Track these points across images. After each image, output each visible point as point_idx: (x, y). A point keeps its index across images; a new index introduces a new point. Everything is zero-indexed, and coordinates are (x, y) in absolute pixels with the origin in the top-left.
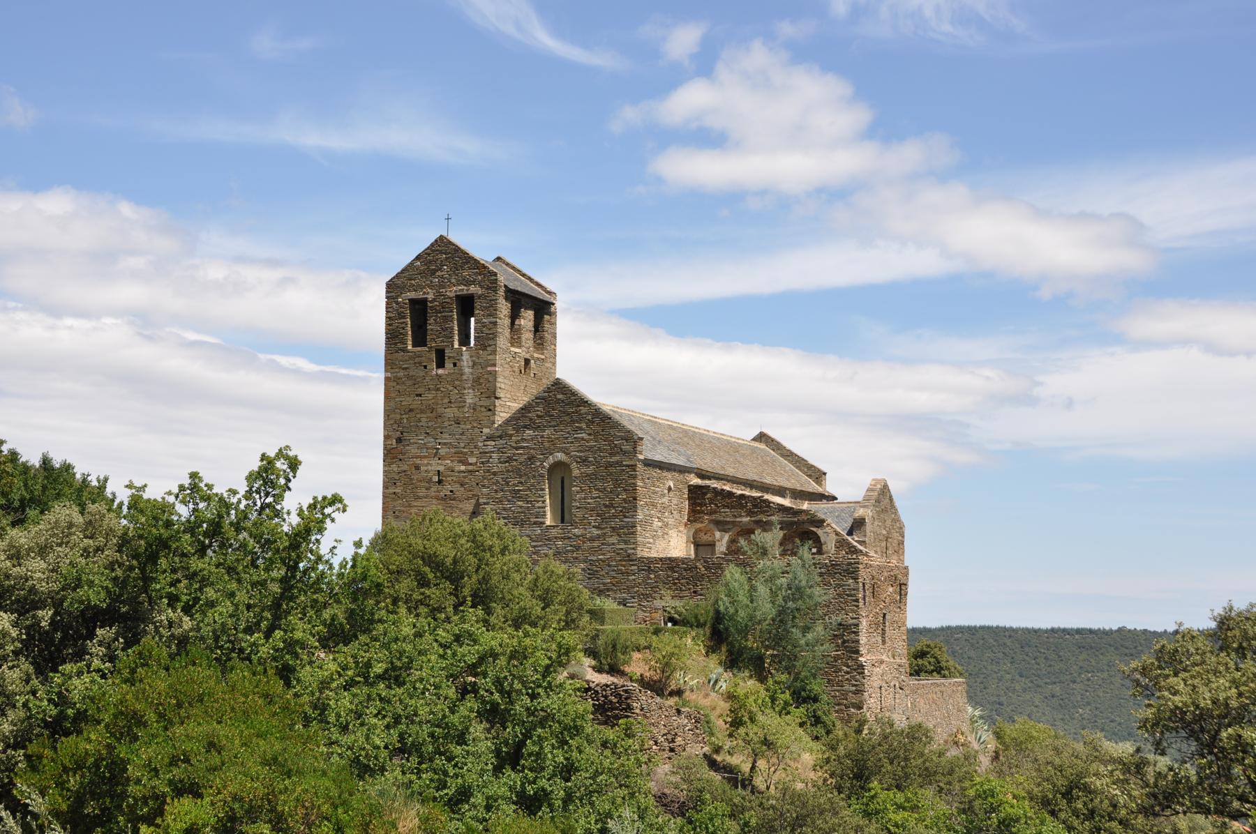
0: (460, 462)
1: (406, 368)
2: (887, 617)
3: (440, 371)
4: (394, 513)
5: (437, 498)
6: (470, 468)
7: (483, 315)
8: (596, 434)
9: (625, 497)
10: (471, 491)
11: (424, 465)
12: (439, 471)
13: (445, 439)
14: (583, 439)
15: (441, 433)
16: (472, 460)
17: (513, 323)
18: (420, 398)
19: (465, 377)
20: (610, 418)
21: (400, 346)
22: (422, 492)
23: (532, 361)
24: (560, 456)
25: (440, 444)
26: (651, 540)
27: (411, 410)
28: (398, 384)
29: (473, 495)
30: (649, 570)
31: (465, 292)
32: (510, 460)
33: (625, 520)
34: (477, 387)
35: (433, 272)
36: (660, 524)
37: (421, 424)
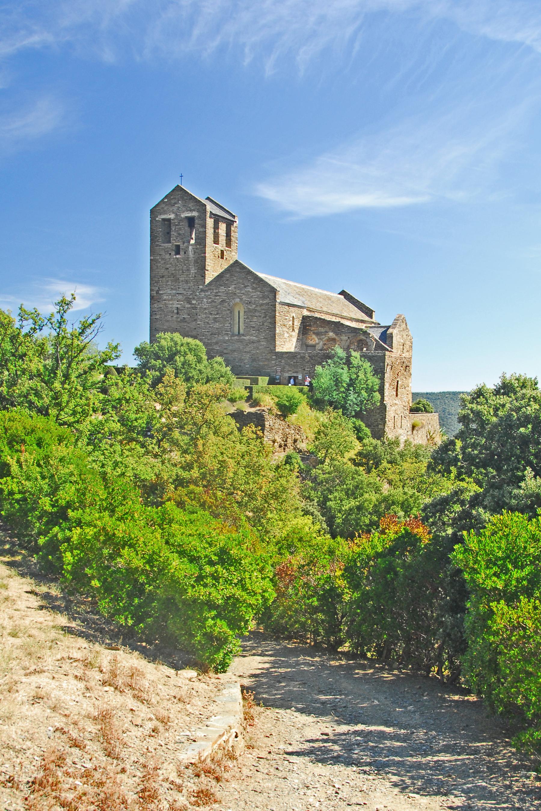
0: (187, 303)
1: (160, 255)
2: (399, 383)
3: (178, 256)
6: (193, 306)
14: (249, 291)
16: (194, 302)
17: (215, 231)
19: (190, 259)
23: (225, 252)
25: (178, 294)
26: (283, 343)
27: (163, 277)
30: (282, 358)
31: (190, 215)
32: (213, 301)
36: (288, 335)
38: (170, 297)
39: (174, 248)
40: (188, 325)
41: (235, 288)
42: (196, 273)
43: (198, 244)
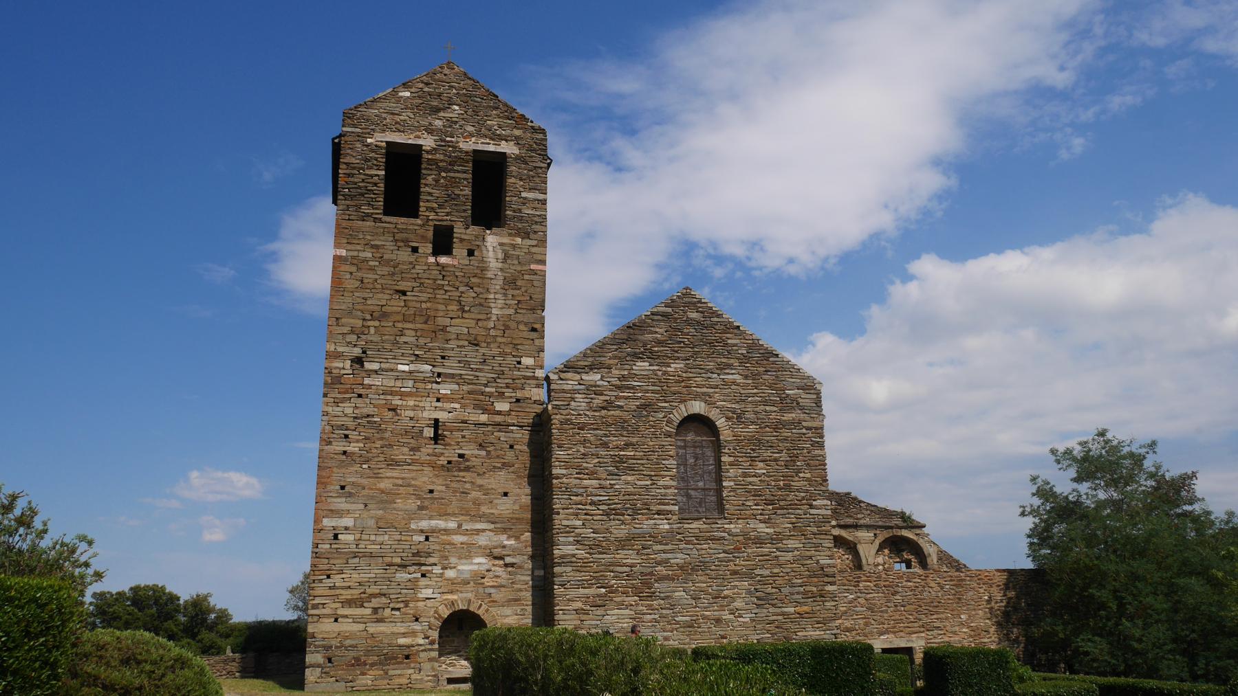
0: (476, 407)
1: (377, 247)
3: (443, 260)
4: (343, 488)
5: (433, 466)
7: (521, 186)
8: (755, 376)
9: (808, 475)
11: (406, 408)
12: (437, 421)
13: (451, 368)
14: (734, 383)
15: (443, 357)
18: (404, 298)
19: (490, 275)
20: (777, 355)
22: (402, 453)
24: (697, 407)
25: (439, 375)
27: (384, 316)
28: (359, 269)
29: (504, 464)
31: (491, 148)
32: (608, 405)
33: (813, 511)
34: (511, 292)
35: (436, 110)
38: (410, 383)
39: (430, 234)
40: (479, 481)
43: (518, 235)
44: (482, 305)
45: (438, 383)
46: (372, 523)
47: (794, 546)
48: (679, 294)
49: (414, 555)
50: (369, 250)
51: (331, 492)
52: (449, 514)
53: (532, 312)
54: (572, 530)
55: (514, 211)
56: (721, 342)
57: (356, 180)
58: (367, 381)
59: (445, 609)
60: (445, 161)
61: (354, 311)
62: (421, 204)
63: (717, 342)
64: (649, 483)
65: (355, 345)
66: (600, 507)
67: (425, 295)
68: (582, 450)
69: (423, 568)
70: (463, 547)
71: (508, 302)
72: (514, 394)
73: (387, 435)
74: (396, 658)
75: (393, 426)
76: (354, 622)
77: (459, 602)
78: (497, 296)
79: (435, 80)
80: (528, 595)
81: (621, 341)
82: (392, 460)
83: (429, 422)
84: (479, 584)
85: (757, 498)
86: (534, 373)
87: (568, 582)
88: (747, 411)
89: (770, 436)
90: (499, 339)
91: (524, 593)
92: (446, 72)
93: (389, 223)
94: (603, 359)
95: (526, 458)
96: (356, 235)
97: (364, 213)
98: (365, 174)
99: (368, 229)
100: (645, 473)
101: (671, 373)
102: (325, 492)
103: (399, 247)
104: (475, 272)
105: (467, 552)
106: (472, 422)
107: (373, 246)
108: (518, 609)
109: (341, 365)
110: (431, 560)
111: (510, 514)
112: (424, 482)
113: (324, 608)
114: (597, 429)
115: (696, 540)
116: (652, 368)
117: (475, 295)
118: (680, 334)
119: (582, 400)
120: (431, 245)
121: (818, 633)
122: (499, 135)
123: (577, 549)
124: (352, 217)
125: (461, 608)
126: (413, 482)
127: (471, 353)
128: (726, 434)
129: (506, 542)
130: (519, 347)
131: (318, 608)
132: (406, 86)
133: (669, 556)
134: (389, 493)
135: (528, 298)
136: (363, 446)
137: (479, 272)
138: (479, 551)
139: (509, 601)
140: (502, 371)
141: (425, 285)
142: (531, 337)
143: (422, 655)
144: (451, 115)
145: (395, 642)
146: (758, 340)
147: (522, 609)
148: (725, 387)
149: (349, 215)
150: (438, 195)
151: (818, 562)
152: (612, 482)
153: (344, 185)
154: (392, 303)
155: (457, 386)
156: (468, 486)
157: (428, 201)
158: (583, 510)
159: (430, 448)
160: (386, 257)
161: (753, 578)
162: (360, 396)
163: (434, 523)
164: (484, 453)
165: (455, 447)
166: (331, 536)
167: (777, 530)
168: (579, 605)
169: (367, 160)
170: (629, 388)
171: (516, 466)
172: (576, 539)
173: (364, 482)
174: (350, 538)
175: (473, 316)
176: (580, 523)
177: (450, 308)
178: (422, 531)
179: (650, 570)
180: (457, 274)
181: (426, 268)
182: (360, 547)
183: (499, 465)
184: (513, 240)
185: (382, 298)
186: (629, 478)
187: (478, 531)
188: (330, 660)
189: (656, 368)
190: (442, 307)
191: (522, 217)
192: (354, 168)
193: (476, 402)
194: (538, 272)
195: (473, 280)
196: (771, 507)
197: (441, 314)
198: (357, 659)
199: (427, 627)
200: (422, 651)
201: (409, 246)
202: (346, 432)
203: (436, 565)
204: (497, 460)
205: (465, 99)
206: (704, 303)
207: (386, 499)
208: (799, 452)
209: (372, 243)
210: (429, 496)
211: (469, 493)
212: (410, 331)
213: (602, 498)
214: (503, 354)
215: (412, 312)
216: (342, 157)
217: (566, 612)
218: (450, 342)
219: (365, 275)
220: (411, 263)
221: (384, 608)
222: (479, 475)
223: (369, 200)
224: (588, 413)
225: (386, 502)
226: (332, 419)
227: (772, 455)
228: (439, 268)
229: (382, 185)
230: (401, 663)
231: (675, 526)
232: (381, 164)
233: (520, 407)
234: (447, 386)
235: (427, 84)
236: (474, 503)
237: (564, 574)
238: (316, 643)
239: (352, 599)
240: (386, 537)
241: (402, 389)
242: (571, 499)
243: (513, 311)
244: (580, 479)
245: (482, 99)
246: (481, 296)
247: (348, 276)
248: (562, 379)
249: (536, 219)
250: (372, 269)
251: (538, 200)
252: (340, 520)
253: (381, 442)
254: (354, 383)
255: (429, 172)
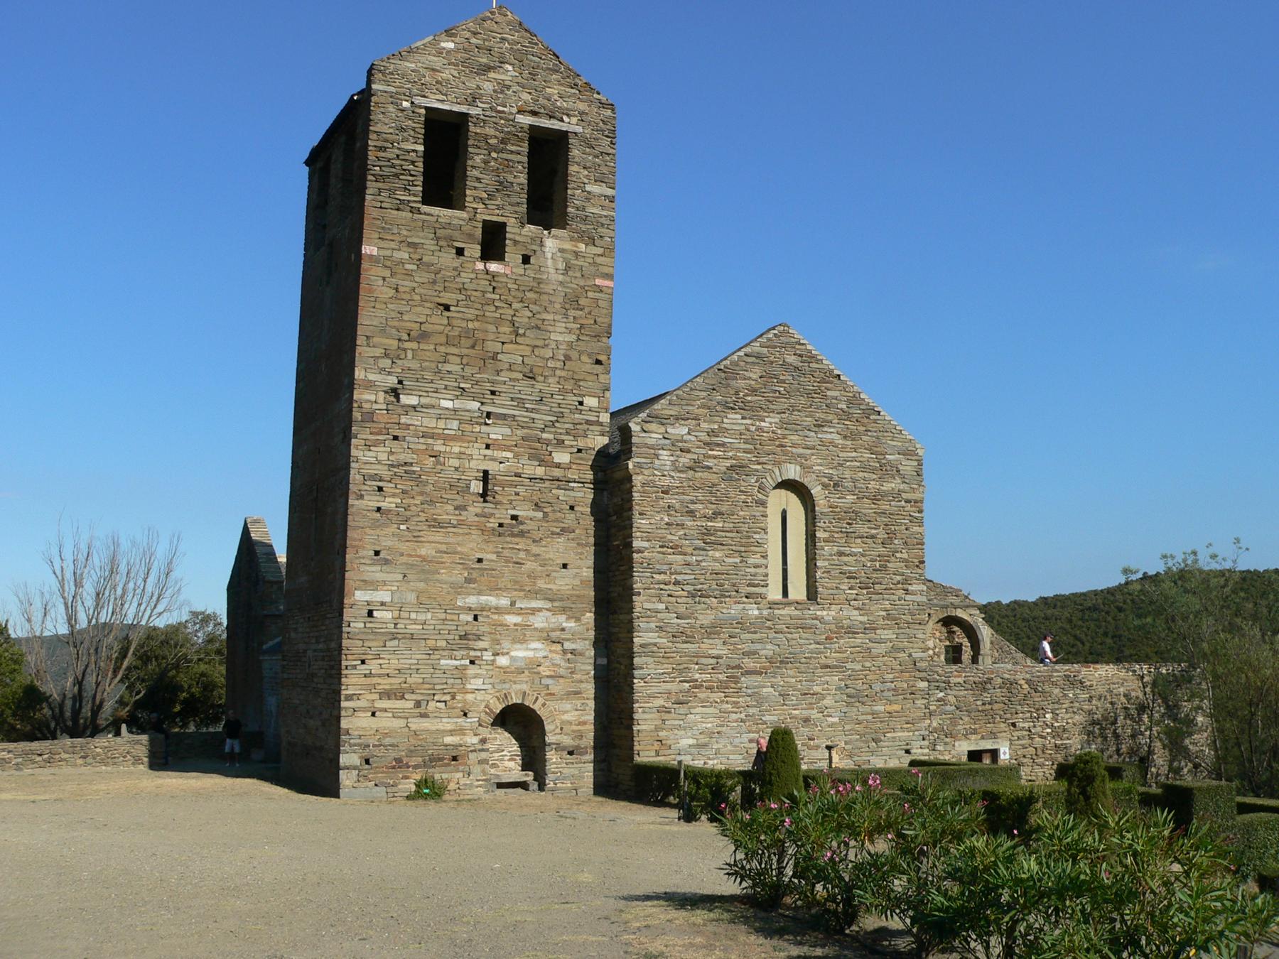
3: (494, 267)
4: (377, 553)
8: (852, 436)
9: (905, 556)
10: (557, 520)
12: (486, 473)
14: (831, 443)
15: (493, 393)
16: (562, 457)
21: (402, 195)
22: (445, 512)
24: (793, 472)
25: (489, 415)
27: (423, 336)
29: (563, 530)
32: (695, 466)
33: (908, 597)
34: (572, 313)
37: (448, 367)
38: (455, 424)
39: (479, 232)
40: (535, 549)
41: (783, 424)
42: (570, 344)
43: (581, 239)
44: (539, 329)
45: (486, 424)
46: (411, 597)
47: (887, 637)
48: (776, 332)
49: (461, 638)
50: (406, 249)
51: (364, 558)
52: (500, 589)
53: (596, 339)
54: (654, 614)
55: (578, 209)
56: (819, 394)
57: (389, 156)
58: (404, 420)
59: (497, 702)
60: (496, 137)
61: (388, 328)
62: (468, 192)
63: (815, 393)
64: (738, 560)
65: (389, 373)
66: (685, 587)
67: (472, 311)
68: (666, 519)
69: (472, 653)
70: (517, 630)
71: (568, 325)
72: (575, 443)
73: (429, 488)
74: (441, 759)
75: (436, 478)
76: (394, 717)
77: (513, 695)
78: (556, 318)
79: (484, 29)
80: (589, 689)
81: (711, 387)
82: (435, 519)
83: (477, 474)
84: (535, 673)
85: (852, 580)
86: (598, 417)
87: (649, 675)
88: (845, 478)
89: (867, 508)
90: (558, 373)
91: (583, 685)
92: (498, 20)
93: (429, 215)
94: (691, 408)
95: (589, 522)
96: (389, 229)
97: (399, 200)
98: (399, 149)
99: (404, 222)
100: (734, 548)
101: (766, 429)
102: (357, 558)
103: (441, 247)
104: (531, 284)
105: (521, 635)
106: (527, 476)
107: (410, 245)
108: (579, 703)
109: (373, 398)
110: (481, 644)
111: (568, 590)
112: (472, 549)
113: (358, 699)
114: (683, 494)
115: (787, 627)
116: (744, 421)
117: (530, 314)
118: (775, 381)
119: (666, 458)
120: (479, 247)
121: (906, 734)
122: (560, 108)
123: (659, 637)
124: (384, 205)
125: (515, 701)
126: (459, 549)
127: (527, 389)
128: (821, 505)
129: (565, 625)
130: (581, 383)
131: (352, 699)
132: (449, 33)
133: (758, 646)
134: (430, 561)
135: (593, 322)
136: (400, 501)
137: (535, 285)
138: (537, 634)
139: (569, 694)
140: (562, 413)
141: (472, 299)
142: (595, 372)
143: (472, 756)
144: (503, 77)
145: (441, 740)
146: (859, 393)
147: (583, 704)
148: (823, 448)
149: (381, 202)
150: (487, 182)
151: (910, 655)
152: (700, 558)
153: (375, 161)
154: (434, 319)
155: (510, 430)
156: (522, 555)
157: (475, 188)
158: (665, 590)
159: (477, 507)
160: (425, 259)
161: (844, 672)
162: (396, 438)
163: (483, 599)
164: (540, 515)
165: (508, 506)
166: (365, 613)
167: (871, 618)
168: (659, 702)
169: (402, 129)
170: (718, 445)
171: (577, 531)
172: (658, 624)
173: (404, 547)
174: (388, 615)
175: (528, 341)
176: (662, 606)
177: (502, 329)
178: (470, 609)
179: (737, 662)
180: (510, 286)
181: (473, 276)
182: (398, 626)
183: (558, 530)
184: (577, 247)
185: (421, 313)
186: (717, 554)
187: (534, 611)
188: (367, 762)
189: (748, 422)
190: (492, 328)
191: (587, 216)
192: (386, 141)
193: (533, 451)
194: (604, 289)
195: (530, 295)
196: (865, 591)
197: (491, 337)
198: (399, 760)
199: (477, 724)
200: (471, 751)
201: (453, 247)
202: (380, 484)
203: (486, 650)
204: (555, 524)
205: (518, 56)
206: (803, 344)
207: (426, 568)
208: (897, 528)
209: (409, 240)
210: (478, 566)
211: (523, 564)
212: (454, 357)
213: (686, 577)
214: (563, 392)
215: (457, 333)
216: (372, 123)
217: (647, 710)
218: (502, 374)
219: (400, 282)
220: (455, 269)
221: (428, 701)
222: (534, 541)
223: (406, 183)
224: (673, 474)
225: (429, 572)
226: (362, 466)
227: (868, 530)
228: (489, 277)
229: (421, 164)
230: (448, 765)
231: (765, 612)
232: (420, 136)
233: (581, 459)
234: (497, 429)
235: (475, 34)
236: (529, 576)
237: (645, 666)
238: (352, 741)
239: (391, 690)
240: (429, 616)
241: (446, 432)
242: (653, 577)
243: (575, 337)
244: (664, 554)
245: (540, 58)
246: (537, 316)
247: (381, 282)
248: (645, 432)
249: (603, 220)
250: (409, 274)
251: (605, 196)
252: (376, 593)
253: (421, 498)
254: (389, 421)
255: (477, 151)
